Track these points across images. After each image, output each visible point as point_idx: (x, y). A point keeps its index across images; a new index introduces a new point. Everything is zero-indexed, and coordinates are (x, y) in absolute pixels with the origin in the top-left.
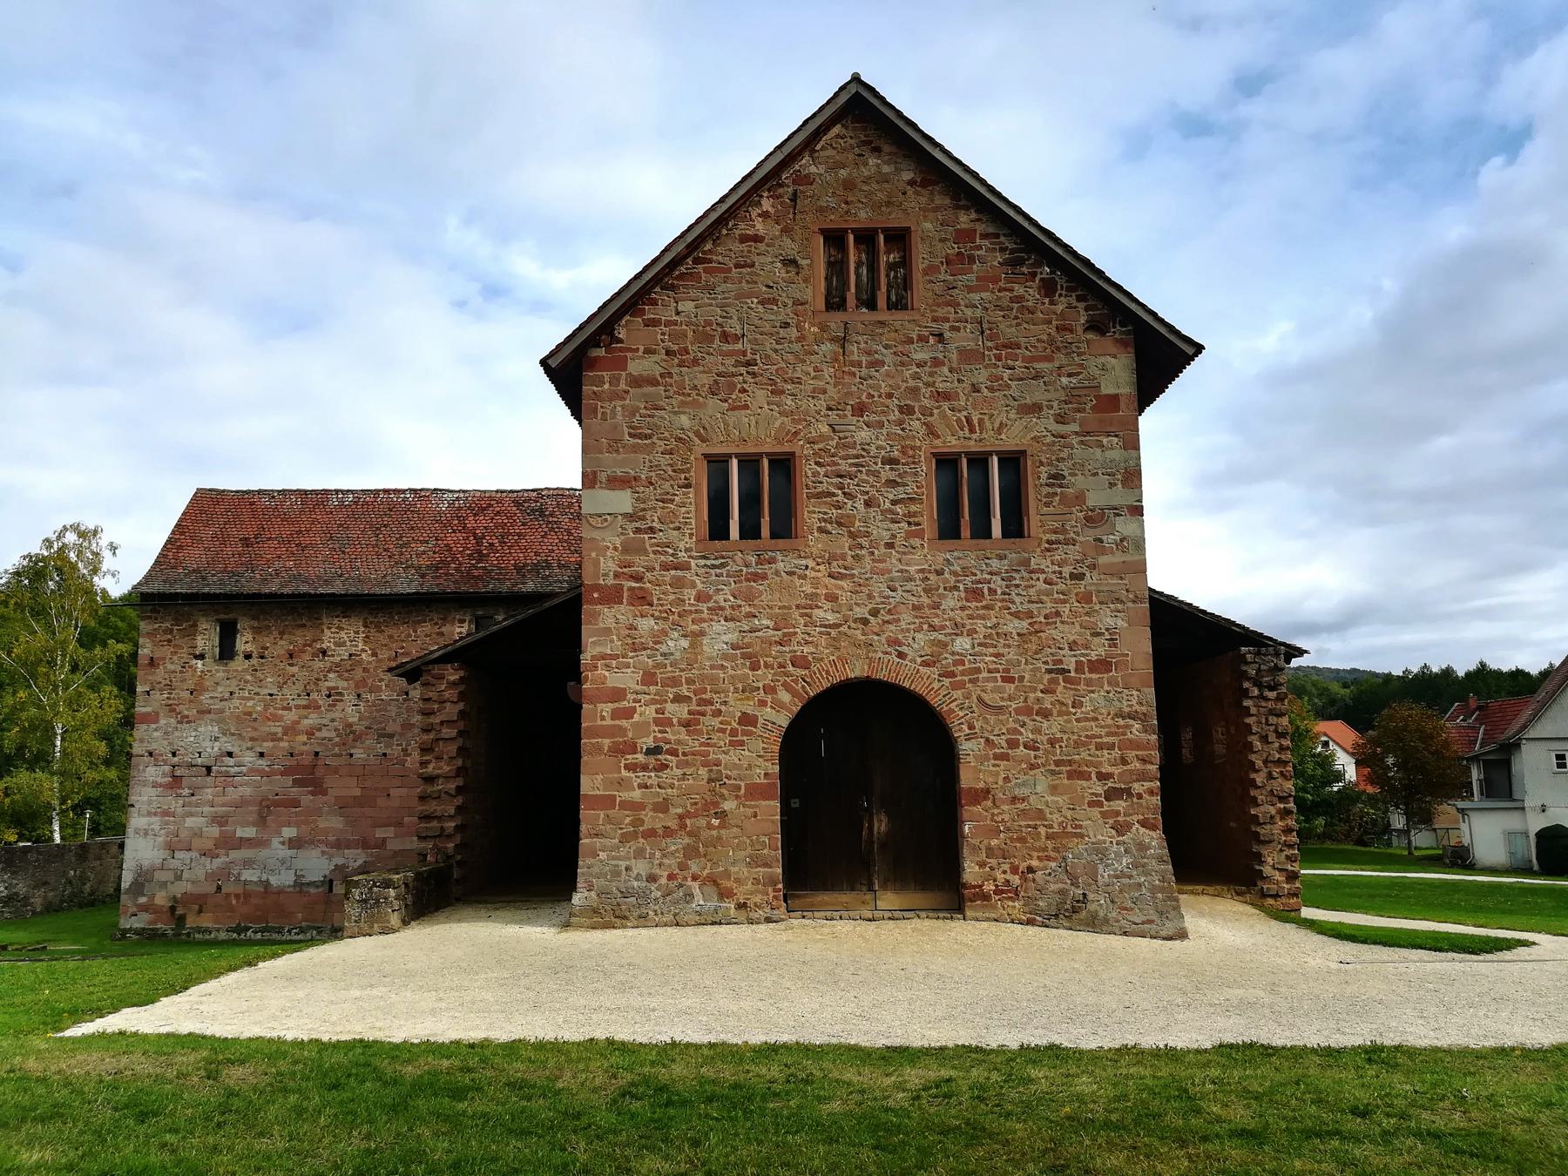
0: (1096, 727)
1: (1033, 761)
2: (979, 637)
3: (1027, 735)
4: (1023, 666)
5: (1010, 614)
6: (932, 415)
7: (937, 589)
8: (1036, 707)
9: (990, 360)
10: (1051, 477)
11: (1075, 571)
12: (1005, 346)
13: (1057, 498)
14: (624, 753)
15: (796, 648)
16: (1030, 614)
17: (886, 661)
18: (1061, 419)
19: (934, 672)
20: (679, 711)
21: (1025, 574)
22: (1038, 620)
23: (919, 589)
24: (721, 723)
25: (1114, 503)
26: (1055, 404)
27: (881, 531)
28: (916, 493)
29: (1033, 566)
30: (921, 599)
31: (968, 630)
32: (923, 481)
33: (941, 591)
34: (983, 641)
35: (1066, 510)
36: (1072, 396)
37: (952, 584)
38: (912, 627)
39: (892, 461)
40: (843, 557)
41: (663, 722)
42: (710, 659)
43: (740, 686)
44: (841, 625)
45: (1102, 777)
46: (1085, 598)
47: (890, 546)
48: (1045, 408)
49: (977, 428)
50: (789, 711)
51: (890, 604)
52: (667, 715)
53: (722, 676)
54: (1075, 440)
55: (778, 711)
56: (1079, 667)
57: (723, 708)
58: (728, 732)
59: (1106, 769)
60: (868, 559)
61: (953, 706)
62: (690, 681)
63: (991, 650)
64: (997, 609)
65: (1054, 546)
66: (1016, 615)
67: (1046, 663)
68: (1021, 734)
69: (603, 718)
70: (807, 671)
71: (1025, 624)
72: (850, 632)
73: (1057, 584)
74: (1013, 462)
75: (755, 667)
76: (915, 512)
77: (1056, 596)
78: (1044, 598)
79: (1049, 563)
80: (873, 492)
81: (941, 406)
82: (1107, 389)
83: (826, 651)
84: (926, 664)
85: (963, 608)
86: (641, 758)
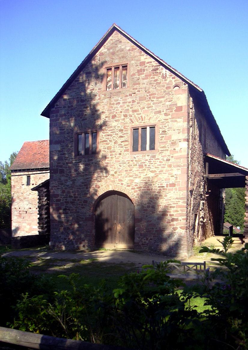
5: (150, 171)
6: (132, 117)
7: (131, 166)
9: (148, 99)
10: (163, 132)
12: (152, 94)
13: (164, 138)
15: (97, 183)
16: (155, 171)
18: (166, 114)
21: (154, 160)
23: (127, 166)
25: (179, 139)
26: (165, 111)
27: (118, 150)
28: (127, 139)
31: (139, 177)
32: (128, 136)
33: (133, 166)
35: (166, 141)
36: (170, 108)
37: (135, 164)
38: (125, 176)
39: (121, 131)
46: (170, 166)
47: (120, 154)
48: (162, 112)
49: (144, 119)
54: (169, 120)
56: (167, 185)
64: (146, 170)
65: (162, 152)
66: (152, 172)
67: (158, 185)
68: (151, 204)
73: (162, 162)
74: (153, 128)
79: (160, 156)
80: (116, 139)
81: (134, 114)
82: (179, 105)
83: (104, 183)
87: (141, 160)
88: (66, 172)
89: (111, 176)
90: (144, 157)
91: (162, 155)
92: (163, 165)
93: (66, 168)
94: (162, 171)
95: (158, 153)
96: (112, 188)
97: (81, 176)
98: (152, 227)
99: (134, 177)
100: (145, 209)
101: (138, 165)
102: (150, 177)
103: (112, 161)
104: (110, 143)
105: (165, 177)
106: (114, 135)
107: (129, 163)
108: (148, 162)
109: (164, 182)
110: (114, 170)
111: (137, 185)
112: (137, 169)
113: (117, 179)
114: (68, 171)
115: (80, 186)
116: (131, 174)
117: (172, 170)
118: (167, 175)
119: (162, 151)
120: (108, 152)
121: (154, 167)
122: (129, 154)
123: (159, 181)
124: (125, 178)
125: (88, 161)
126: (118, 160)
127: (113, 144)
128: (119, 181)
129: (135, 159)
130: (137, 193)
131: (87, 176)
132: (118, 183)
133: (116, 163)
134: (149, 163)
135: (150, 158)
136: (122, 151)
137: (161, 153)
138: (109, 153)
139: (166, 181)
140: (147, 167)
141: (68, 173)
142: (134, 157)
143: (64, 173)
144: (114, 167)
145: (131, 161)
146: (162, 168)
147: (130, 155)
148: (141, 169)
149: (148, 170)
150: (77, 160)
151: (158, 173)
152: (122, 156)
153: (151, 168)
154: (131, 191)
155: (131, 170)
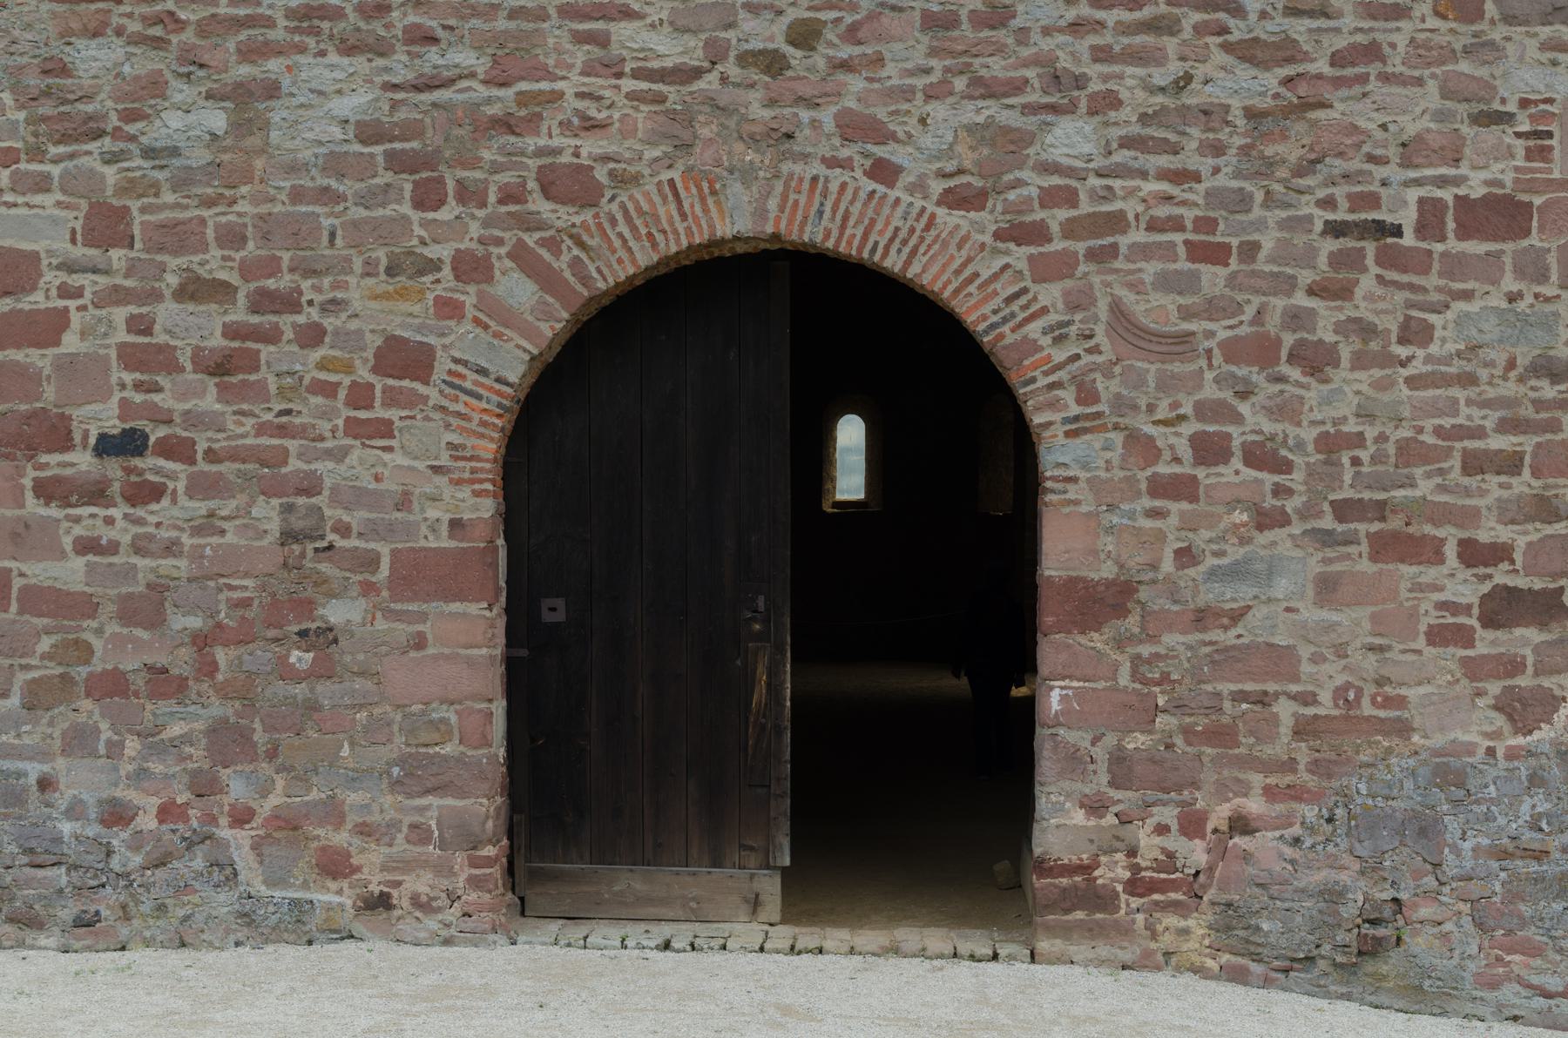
2: (1126, 119)
4: (1257, 212)
5: (1227, 47)
16: (1287, 51)
17: (834, 187)
22: (1312, 68)
31: (1092, 97)
34: (1136, 129)
38: (920, 82)
61: (1034, 329)
63: (1164, 161)
66: (1249, 53)
67: (1328, 203)
71: (1271, 79)
84: (956, 199)
85: (1076, 27)
89: (755, 75)
99: (1033, 97)
102: (1226, 108)
109: (1393, 172)
113: (827, 116)
116: (997, 68)
123: (1338, 165)
128: (846, 139)
132: (831, 163)
149: (1199, 29)
151: (1319, 77)
154: (999, 262)
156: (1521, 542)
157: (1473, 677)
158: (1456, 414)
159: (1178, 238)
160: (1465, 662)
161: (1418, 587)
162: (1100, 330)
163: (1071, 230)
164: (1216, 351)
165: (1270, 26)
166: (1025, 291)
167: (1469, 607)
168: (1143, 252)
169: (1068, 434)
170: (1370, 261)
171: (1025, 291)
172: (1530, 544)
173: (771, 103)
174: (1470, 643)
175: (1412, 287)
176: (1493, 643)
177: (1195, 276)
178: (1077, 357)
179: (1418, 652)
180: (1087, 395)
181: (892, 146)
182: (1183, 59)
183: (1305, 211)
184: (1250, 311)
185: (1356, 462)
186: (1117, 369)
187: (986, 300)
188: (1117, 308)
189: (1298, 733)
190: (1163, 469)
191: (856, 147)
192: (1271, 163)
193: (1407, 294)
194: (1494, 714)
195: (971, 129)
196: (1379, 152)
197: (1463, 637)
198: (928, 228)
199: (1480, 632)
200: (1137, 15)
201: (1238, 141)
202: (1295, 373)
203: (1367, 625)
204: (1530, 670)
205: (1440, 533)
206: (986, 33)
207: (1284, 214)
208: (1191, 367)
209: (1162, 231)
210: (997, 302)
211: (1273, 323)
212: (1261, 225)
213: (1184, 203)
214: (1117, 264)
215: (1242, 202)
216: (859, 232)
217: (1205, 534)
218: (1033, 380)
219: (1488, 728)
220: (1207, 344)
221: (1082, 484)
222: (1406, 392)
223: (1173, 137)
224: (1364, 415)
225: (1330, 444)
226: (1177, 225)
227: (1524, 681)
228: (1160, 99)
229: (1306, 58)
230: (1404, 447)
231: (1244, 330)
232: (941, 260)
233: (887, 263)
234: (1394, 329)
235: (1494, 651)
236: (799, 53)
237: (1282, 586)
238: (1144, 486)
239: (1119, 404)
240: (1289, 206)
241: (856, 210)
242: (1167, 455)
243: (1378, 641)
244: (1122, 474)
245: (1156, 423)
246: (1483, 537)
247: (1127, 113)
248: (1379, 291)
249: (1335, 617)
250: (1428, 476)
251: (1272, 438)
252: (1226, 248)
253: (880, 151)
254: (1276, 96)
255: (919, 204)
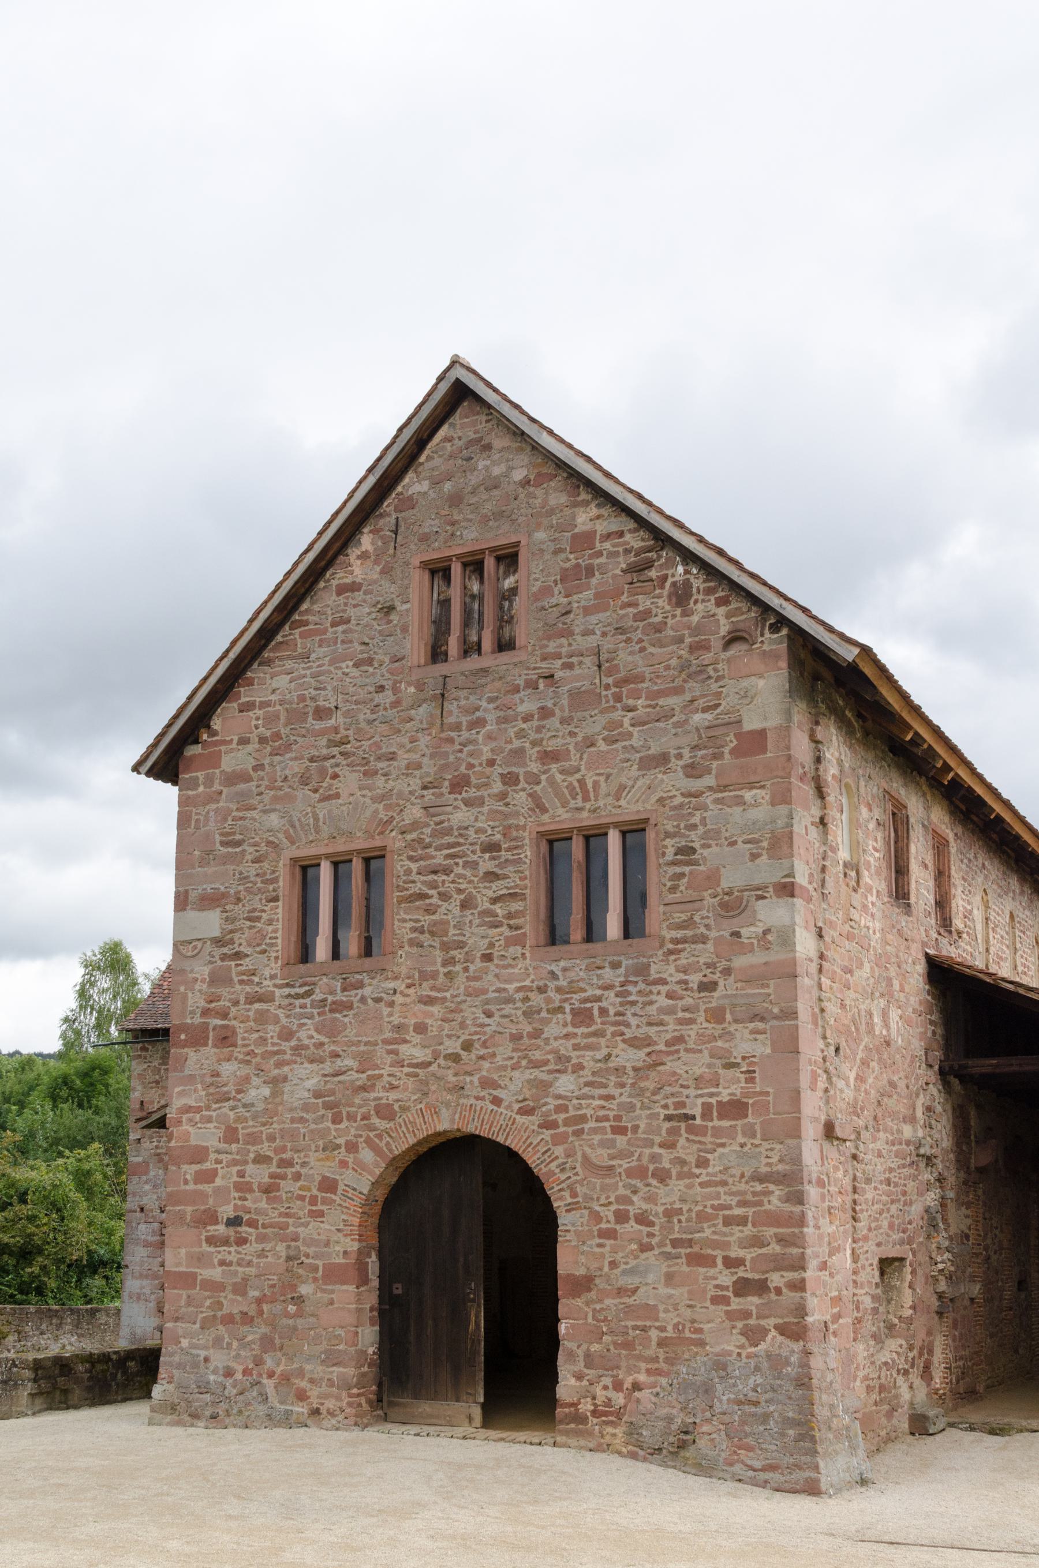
0: (725, 1193)
1: (646, 1240)
2: (587, 1075)
3: (639, 1204)
4: (638, 1112)
5: (624, 1041)
7: (539, 1012)
8: (651, 1167)
11: (705, 980)
14: (205, 1225)
15: (381, 1094)
16: (646, 1042)
17: (478, 1108)
19: (532, 1122)
20: (258, 1174)
21: (641, 986)
22: (657, 1048)
23: (519, 1013)
24: (300, 1189)
27: (477, 938)
28: (517, 886)
29: (654, 975)
30: (520, 1026)
31: (573, 1065)
33: (544, 1014)
34: (590, 1078)
37: (557, 1004)
38: (509, 1063)
40: (434, 975)
41: (244, 1188)
42: (291, 1110)
43: (321, 1143)
44: (430, 1064)
45: (731, 1263)
47: (487, 958)
50: (371, 1173)
51: (485, 1033)
52: (248, 1179)
53: (302, 1131)
55: (360, 1174)
57: (303, 1171)
58: (307, 1200)
59: (735, 1252)
60: (462, 978)
62: (272, 1138)
64: (609, 1036)
66: (634, 1043)
67: (665, 1107)
68: (632, 1203)
69: (186, 1182)
70: (392, 1124)
71: (642, 1054)
72: (441, 1073)
73: (682, 998)
75: (337, 1120)
76: (517, 912)
77: (680, 1015)
78: (666, 1018)
79: (672, 969)
84: (525, 1111)
85: (567, 1036)
86: (221, 1229)
87: (582, 985)
88: (244, 1039)
90: (599, 972)
91: (679, 962)
92: (683, 1011)
93: (247, 1019)
94: (680, 1039)
95: (660, 952)
96: (453, 1121)
97: (312, 1062)
98: (639, 1323)
99: (552, 1066)
100: (609, 1226)
101: (568, 1008)
102: (625, 1067)
103: (451, 991)
104: (439, 906)
105: (698, 1071)
106: (459, 870)
107: (526, 999)
108: (617, 995)
110: (460, 1033)
111: (564, 1109)
112: (565, 1031)
113: (475, 1079)
114: (255, 1036)
115: (306, 1107)
116: (537, 1055)
117: (730, 1033)
118: (705, 1058)
119: (676, 941)
120: (431, 946)
121: (644, 1020)
122: (528, 955)
123: (668, 1090)
124: (509, 1073)
125: (344, 990)
126: (477, 984)
127: (457, 911)
128: (483, 1088)
129: (556, 983)
130: (566, 1146)
131: (339, 1062)
132: (477, 1098)
133: (469, 999)
134: (619, 1000)
135: (626, 976)
136: (497, 944)
137: (671, 952)
138: (438, 952)
139: (700, 1092)
140: (612, 1019)
141: (252, 1047)
142: (552, 973)
143: (235, 1045)
144: (458, 1017)
145: (536, 992)
146: (678, 1028)
147: (534, 964)
148: (579, 1031)
149: (614, 1034)
150: (293, 986)
151: (661, 1051)
152: (497, 966)
153: (628, 1025)
155: (536, 1034)
156: (748, 1257)
157: (731, 1320)
158: (719, 1198)
159: (607, 1124)
160: (727, 1312)
161: (706, 1278)
162: (578, 1165)
163: (567, 1122)
164: (623, 1174)
165: (641, 1031)
166: (549, 1149)
167: (728, 1287)
168: (594, 1131)
169: (568, 1211)
170: (683, 1131)
171: (549, 1149)
172: (752, 1258)
173: (456, 1074)
174: (729, 1304)
175: (700, 1142)
176: (739, 1304)
177: (614, 1141)
178: (569, 1177)
179: (707, 1308)
180: (574, 1195)
181: (500, 1090)
182: (608, 1047)
183: (657, 1110)
184: (637, 1155)
185: (680, 1221)
186: (585, 1182)
187: (535, 1154)
188: (585, 1157)
189: (660, 1344)
190: (604, 1226)
191: (487, 1091)
192: (643, 1090)
193: (698, 1146)
194: (740, 1337)
195: (529, 1081)
196: (685, 1083)
197: (726, 1301)
198: (513, 1124)
199: (733, 1299)
200: (590, 1030)
201: (630, 1081)
202: (654, 1182)
203: (686, 1295)
204: (754, 1316)
205: (714, 1253)
206: (534, 1041)
207: (648, 1112)
208: (614, 1181)
209: (601, 1122)
210: (539, 1155)
211: (645, 1160)
212: (639, 1118)
213: (609, 1109)
214: (584, 1137)
215: (632, 1108)
216: (488, 1127)
217: (621, 1254)
218: (553, 1188)
219: (738, 1344)
220: (619, 1170)
221: (572, 1233)
222: (699, 1189)
223: (604, 1081)
224: (683, 1200)
225: (670, 1214)
226: (606, 1119)
227: (752, 1322)
228: (599, 1065)
229: (655, 1043)
230: (699, 1214)
231: (634, 1164)
232: (518, 1137)
233: (498, 1140)
234: (694, 1161)
235: (738, 1307)
236: (466, 1053)
237: (651, 1278)
238: (596, 1233)
239: (588, 1198)
240: (650, 1108)
241: (486, 1118)
242: (605, 1220)
243: (691, 1303)
244: (587, 1228)
245: (601, 1205)
246: (733, 1255)
247: (586, 1072)
248: (687, 1145)
249: (673, 1292)
250: (709, 1227)
251: (646, 1211)
252: (626, 1128)
253: (495, 1093)
254: (644, 1061)
255: (509, 1114)
